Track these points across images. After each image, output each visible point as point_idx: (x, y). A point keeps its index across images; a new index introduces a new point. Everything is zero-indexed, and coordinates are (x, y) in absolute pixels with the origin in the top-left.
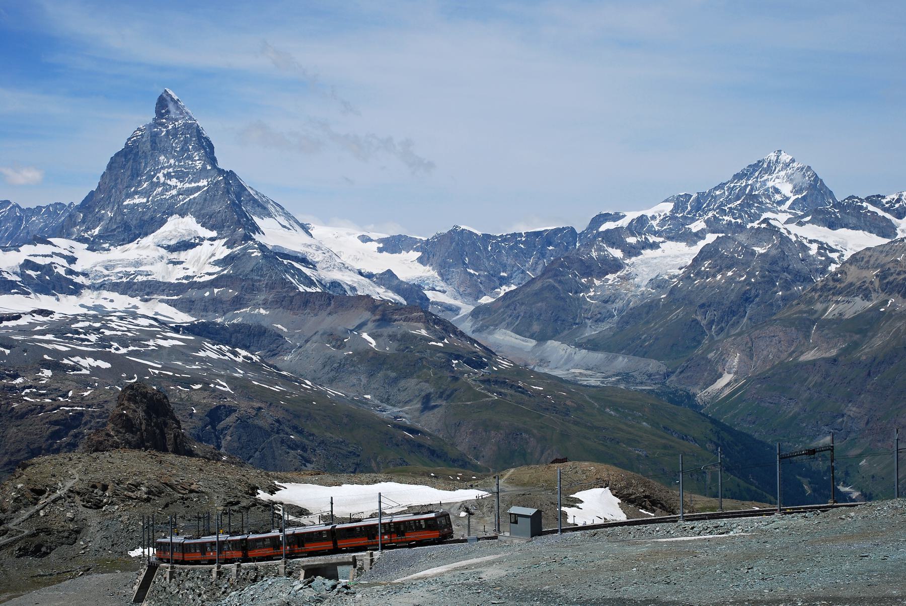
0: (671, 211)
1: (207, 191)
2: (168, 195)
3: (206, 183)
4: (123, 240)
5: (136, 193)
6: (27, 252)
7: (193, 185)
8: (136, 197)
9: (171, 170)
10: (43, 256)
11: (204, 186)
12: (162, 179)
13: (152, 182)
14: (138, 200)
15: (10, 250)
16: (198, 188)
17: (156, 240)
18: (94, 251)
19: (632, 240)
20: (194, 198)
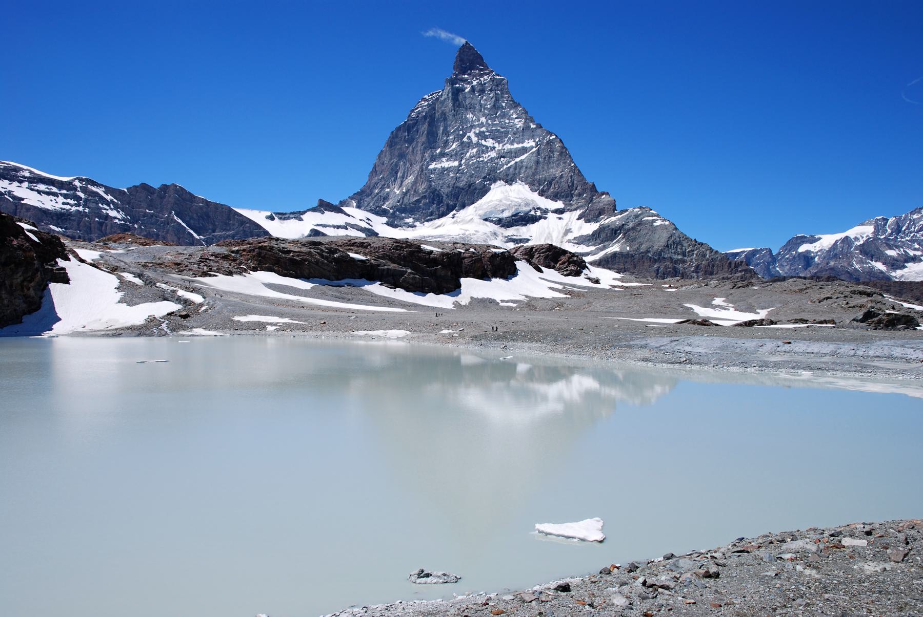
0: (874, 233)
1: (538, 152)
2: (486, 157)
3: (533, 144)
4: (431, 214)
5: (443, 155)
6: (311, 220)
7: (516, 146)
8: (444, 159)
9: (484, 129)
10: (334, 227)
11: (532, 147)
12: (475, 140)
13: (462, 143)
14: (446, 164)
15: (288, 218)
16: (525, 150)
17: (481, 212)
18: (395, 226)
19: (891, 253)
20: (522, 161)
